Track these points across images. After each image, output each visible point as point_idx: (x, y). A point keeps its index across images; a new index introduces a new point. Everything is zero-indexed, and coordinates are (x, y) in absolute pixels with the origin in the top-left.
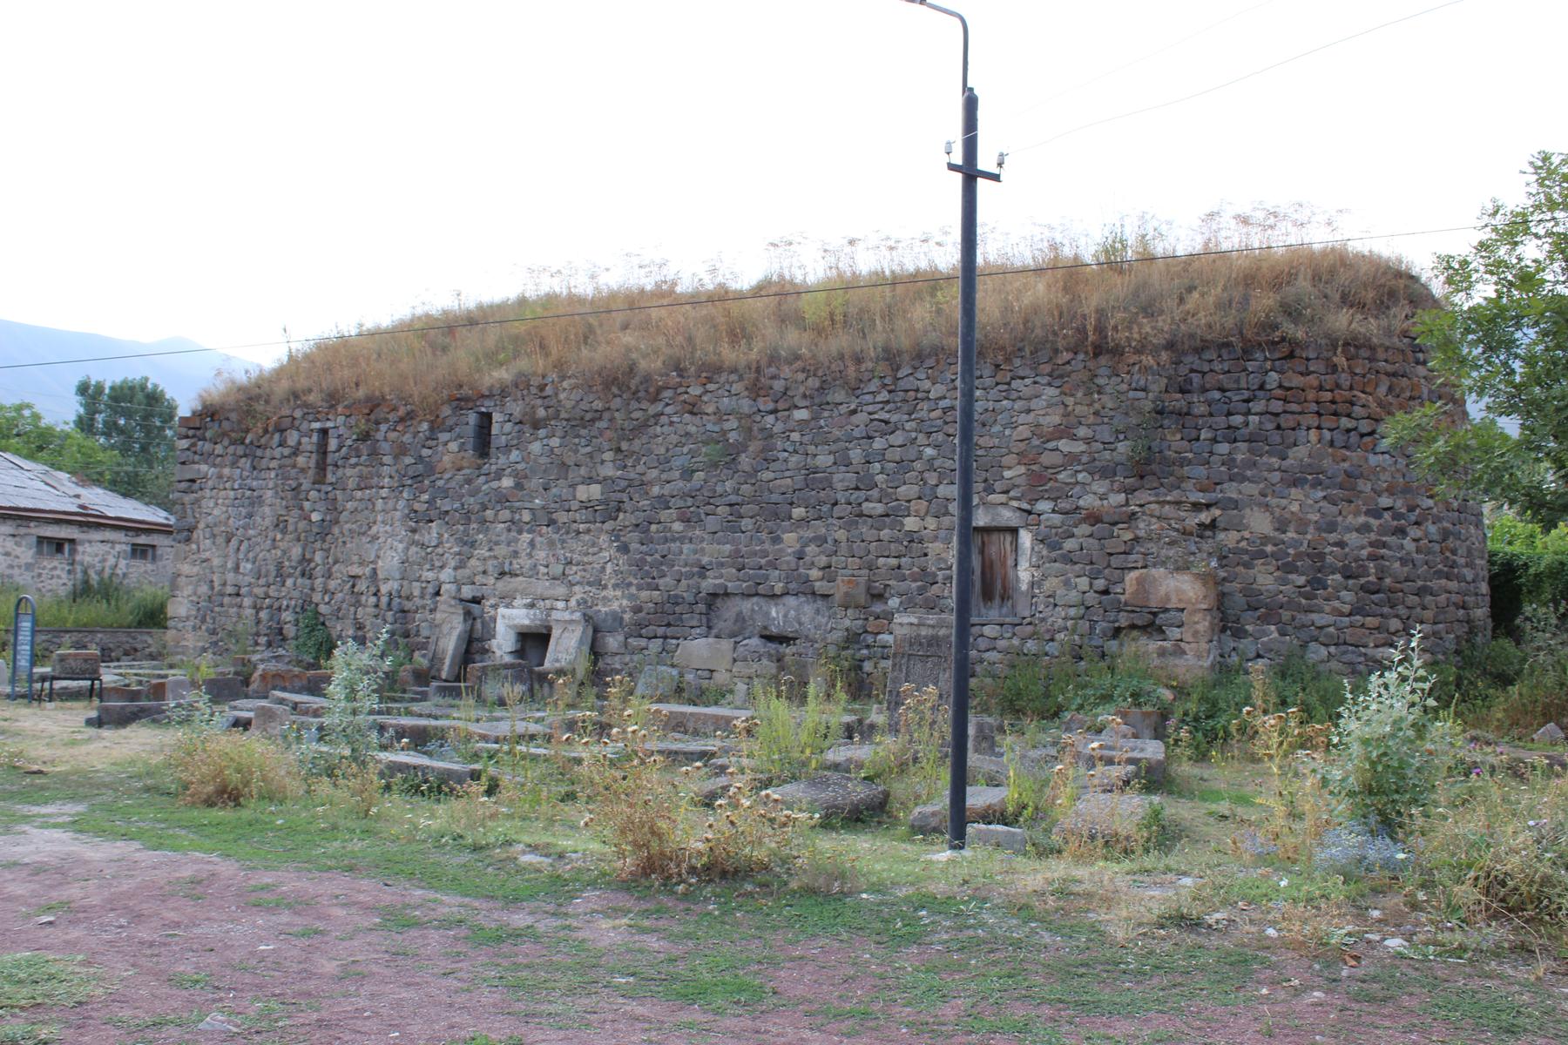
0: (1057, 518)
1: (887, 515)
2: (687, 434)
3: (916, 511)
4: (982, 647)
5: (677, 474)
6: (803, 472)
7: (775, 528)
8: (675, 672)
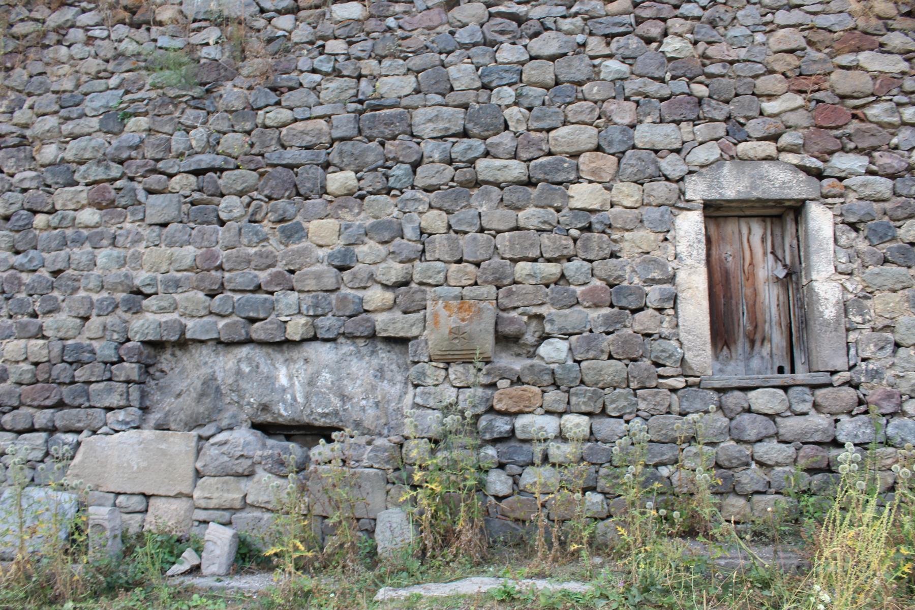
0: (883, 186)
1: (530, 183)
2: (119, 56)
3: (593, 172)
4: (751, 433)
5: (95, 123)
6: (353, 106)
7: (291, 210)
8: (67, 499)
